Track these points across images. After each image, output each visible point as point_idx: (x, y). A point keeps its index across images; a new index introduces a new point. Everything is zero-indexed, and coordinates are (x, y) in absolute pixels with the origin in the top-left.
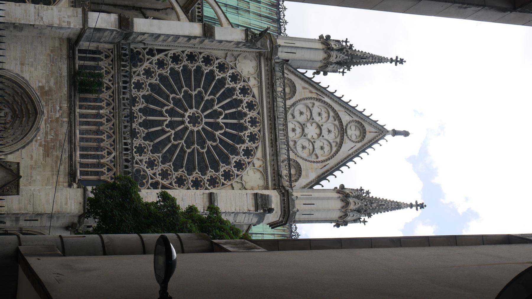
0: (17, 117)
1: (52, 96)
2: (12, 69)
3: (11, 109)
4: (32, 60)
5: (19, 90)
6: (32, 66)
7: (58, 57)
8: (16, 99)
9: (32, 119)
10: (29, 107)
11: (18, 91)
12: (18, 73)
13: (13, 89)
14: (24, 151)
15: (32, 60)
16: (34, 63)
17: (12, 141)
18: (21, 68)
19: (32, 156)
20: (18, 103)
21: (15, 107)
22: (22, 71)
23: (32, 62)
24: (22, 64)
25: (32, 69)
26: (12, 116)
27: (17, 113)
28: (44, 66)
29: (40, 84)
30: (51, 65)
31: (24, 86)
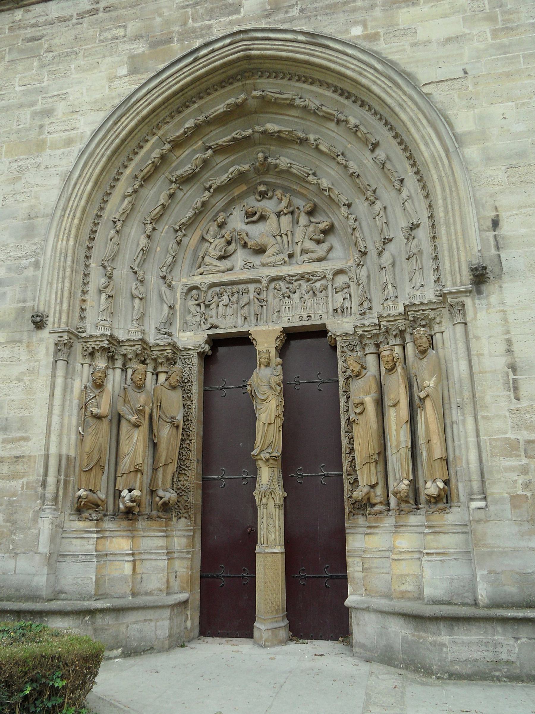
0: (265, 168)
1: (167, 22)
2: (57, 181)
3: (231, 203)
4: (26, 115)
5: (151, 150)
6: (48, 113)
7: (18, 36)
8: (187, 168)
9: (270, 87)
10: (221, 108)
11: (156, 154)
12: (76, 154)
13: (147, 179)
14: (423, 75)
15: (26, 115)
16: (38, 107)
17: (375, 146)
18: (54, 146)
19: (449, 40)
20: (205, 162)
21: (224, 178)
22: (69, 142)
23: (35, 114)
24: (41, 146)
25: (61, 107)
26: (263, 195)
27: (246, 167)
28: (50, 73)
29: (124, 71)
30: (49, 51)
31: (129, 123)
